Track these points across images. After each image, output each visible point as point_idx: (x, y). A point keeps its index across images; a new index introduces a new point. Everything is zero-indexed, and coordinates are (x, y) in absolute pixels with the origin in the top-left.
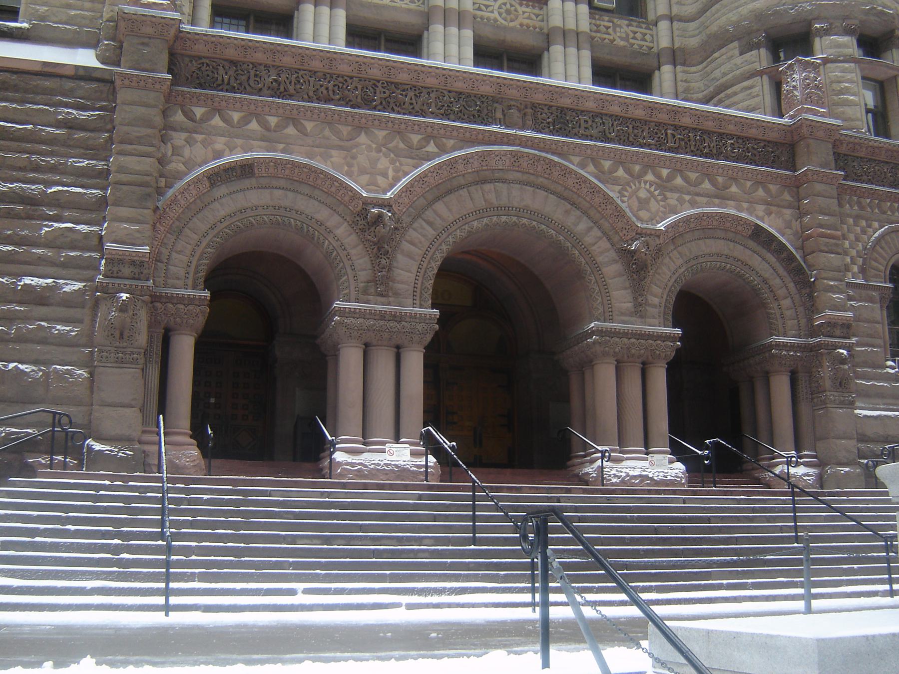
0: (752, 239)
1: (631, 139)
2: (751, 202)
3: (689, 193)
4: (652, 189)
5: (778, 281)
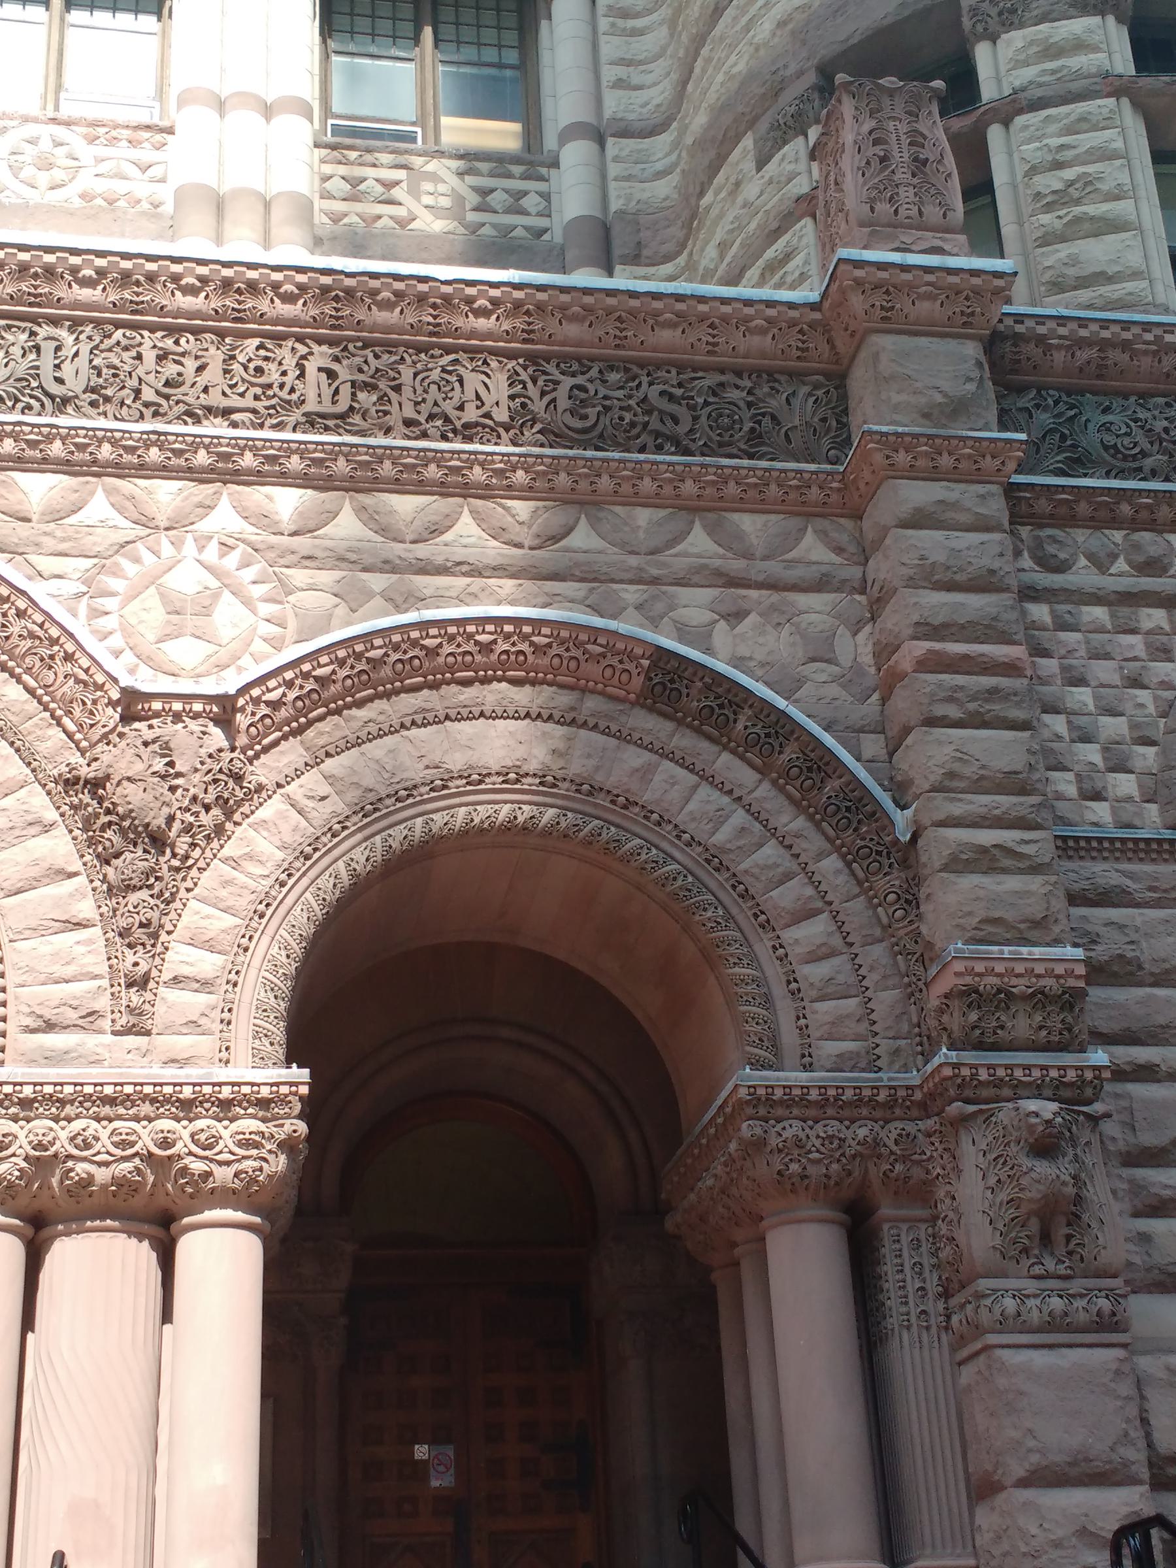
0: (651, 710)
1: (148, 395)
2: (655, 581)
3: (388, 566)
4: (232, 560)
5: (770, 851)
